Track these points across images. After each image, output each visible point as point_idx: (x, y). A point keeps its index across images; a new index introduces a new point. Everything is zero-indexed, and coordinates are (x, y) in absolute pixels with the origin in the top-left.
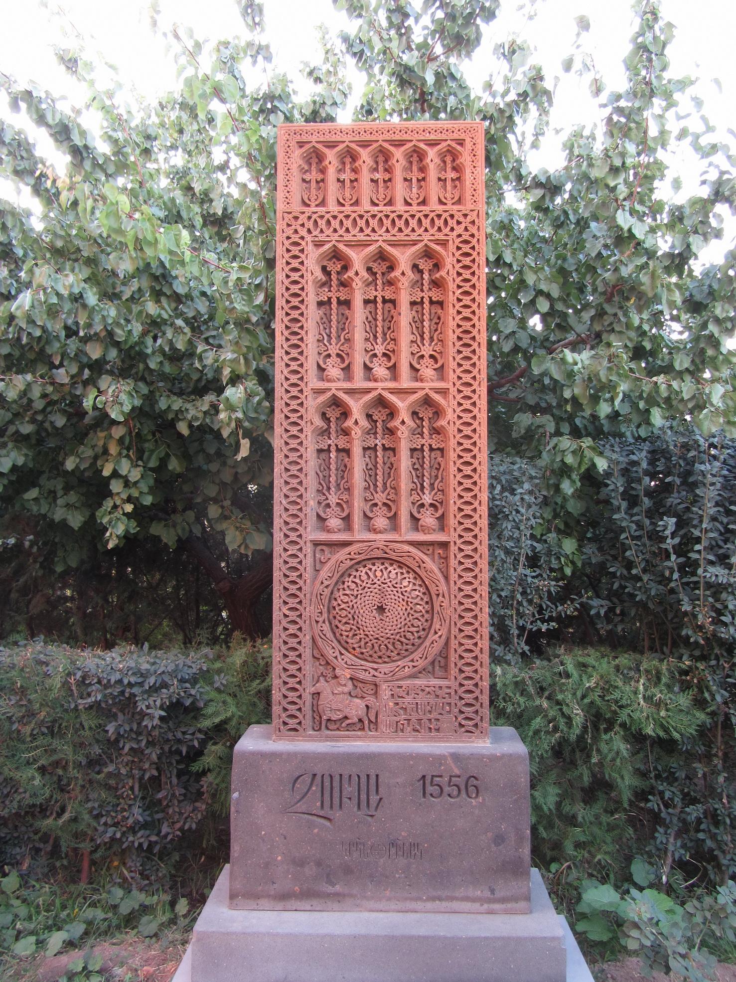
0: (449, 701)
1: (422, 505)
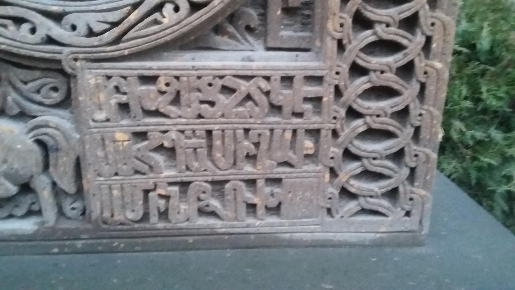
0: (313, 121)
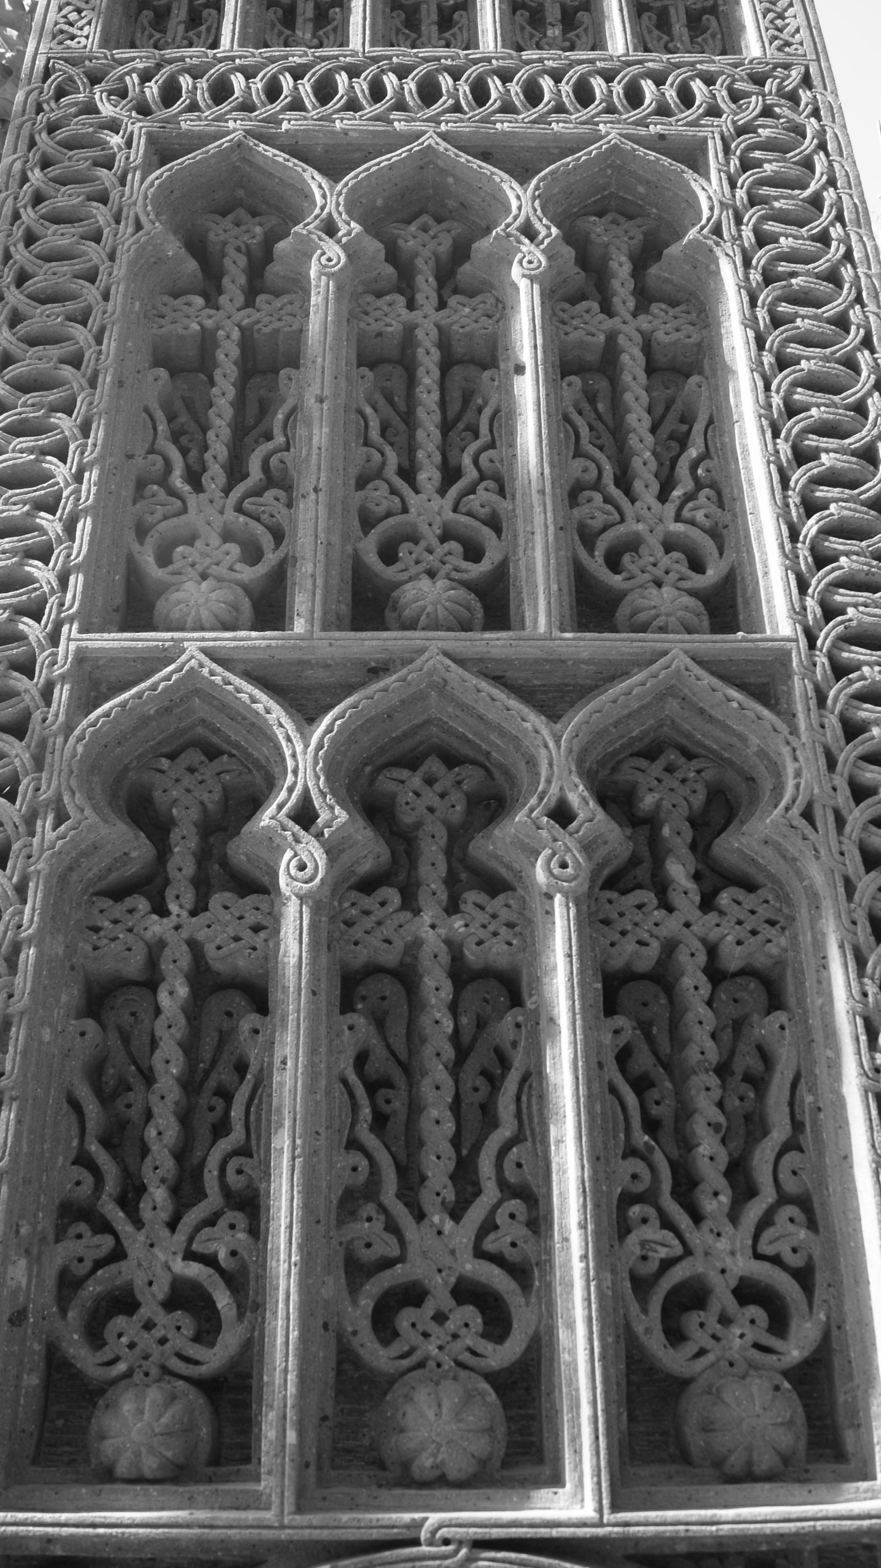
1: (691, 1297)
